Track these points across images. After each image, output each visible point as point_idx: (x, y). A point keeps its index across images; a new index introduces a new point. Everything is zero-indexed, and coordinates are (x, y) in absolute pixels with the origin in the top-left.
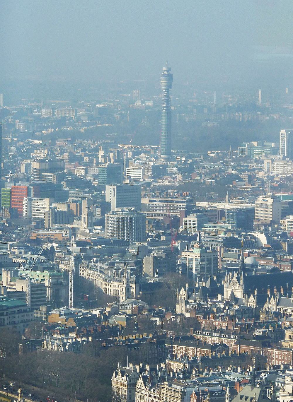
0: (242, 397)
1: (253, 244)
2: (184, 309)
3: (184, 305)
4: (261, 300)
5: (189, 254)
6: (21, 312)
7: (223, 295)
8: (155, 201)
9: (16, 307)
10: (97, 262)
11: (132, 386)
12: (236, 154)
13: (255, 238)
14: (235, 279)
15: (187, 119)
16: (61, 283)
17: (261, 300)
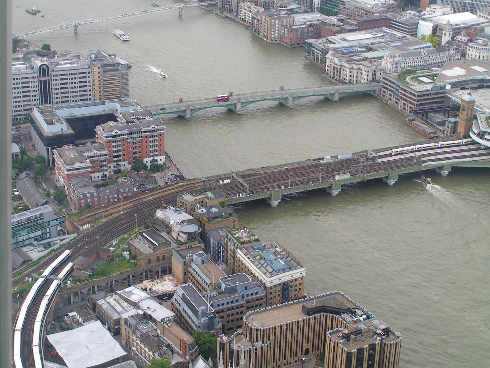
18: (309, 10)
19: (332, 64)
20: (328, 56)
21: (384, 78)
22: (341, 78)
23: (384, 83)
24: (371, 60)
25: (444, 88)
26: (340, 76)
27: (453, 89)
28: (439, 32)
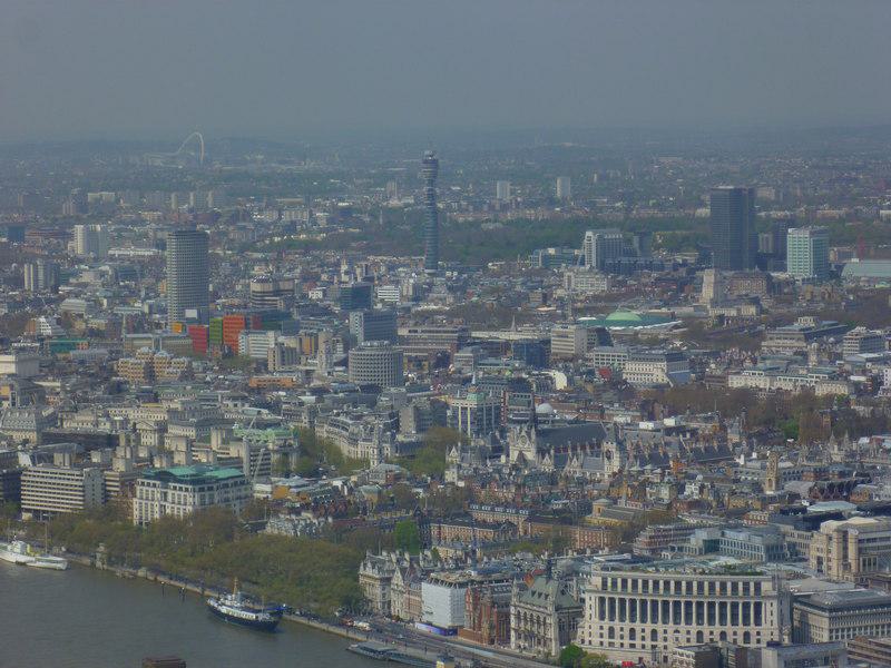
0: (534, 593)
1: (546, 386)
2: (455, 476)
3: (455, 470)
4: (560, 462)
5: (462, 401)
6: (236, 484)
7: (508, 456)
8: (416, 331)
9: (228, 478)
10: (338, 415)
11: (386, 581)
12: (526, 266)
13: (551, 378)
14: (523, 433)
15: (461, 220)
16: (290, 445)
17: (560, 462)
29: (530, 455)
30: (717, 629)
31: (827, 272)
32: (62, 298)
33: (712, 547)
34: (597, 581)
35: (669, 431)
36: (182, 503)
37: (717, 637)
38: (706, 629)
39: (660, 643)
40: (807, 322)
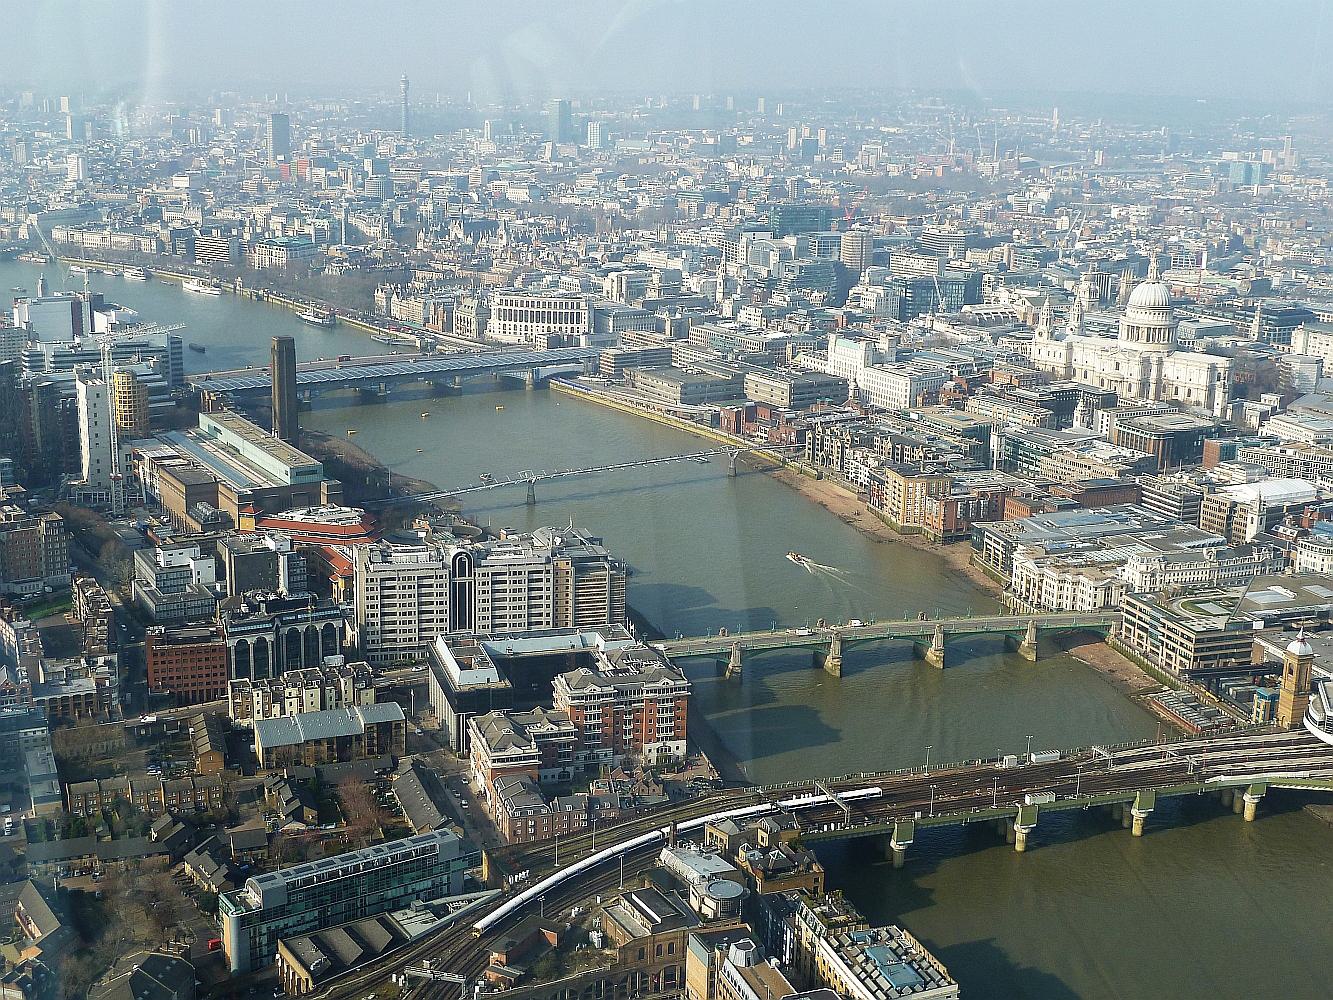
1: (470, 201)
4: (476, 241)
11: (389, 299)
17: (476, 241)
18: (982, 465)
19: (1025, 572)
20: (1015, 555)
21: (1128, 603)
22: (1043, 600)
23: (1127, 612)
24: (1103, 566)
25: (1249, 626)
26: (1039, 597)
27: (1268, 629)
28: (1241, 516)
29: (460, 236)
30: (558, 325)
31: (605, 145)
32: (211, 148)
33: (555, 284)
34: (497, 300)
35: (531, 225)
36: (280, 257)
37: (557, 330)
38: (552, 325)
39: (529, 332)
40: (599, 171)
